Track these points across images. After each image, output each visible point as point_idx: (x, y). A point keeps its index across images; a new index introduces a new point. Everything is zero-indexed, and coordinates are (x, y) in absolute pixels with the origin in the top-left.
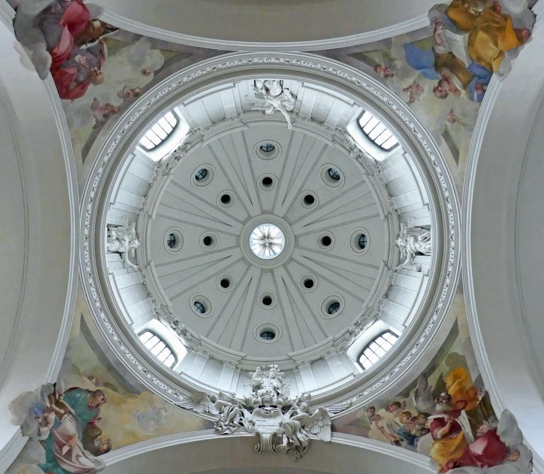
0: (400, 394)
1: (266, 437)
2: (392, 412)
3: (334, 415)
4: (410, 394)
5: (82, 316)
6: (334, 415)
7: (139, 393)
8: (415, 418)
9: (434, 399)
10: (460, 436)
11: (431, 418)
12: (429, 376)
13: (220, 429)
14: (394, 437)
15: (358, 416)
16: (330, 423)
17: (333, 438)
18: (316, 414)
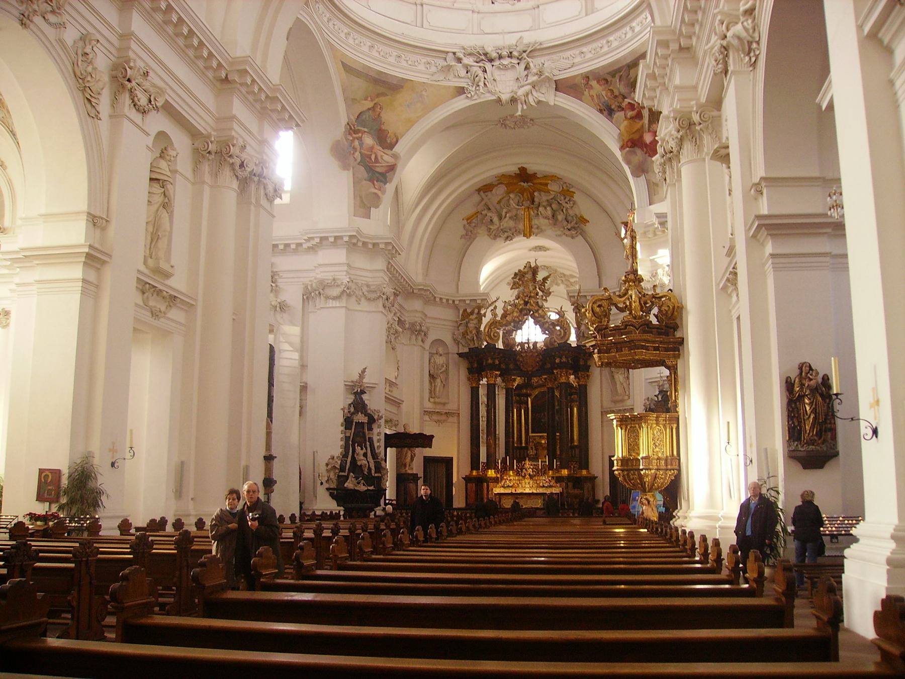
0: (609, 73)
1: (505, 97)
2: (600, 85)
3: (558, 73)
4: (617, 76)
5: (342, 62)
6: (558, 73)
7: (402, 87)
8: (616, 97)
9: (632, 88)
10: (641, 124)
11: (627, 101)
12: (632, 68)
13: (469, 95)
14: (600, 106)
15: (576, 81)
16: (555, 87)
17: (557, 99)
18: (544, 78)
